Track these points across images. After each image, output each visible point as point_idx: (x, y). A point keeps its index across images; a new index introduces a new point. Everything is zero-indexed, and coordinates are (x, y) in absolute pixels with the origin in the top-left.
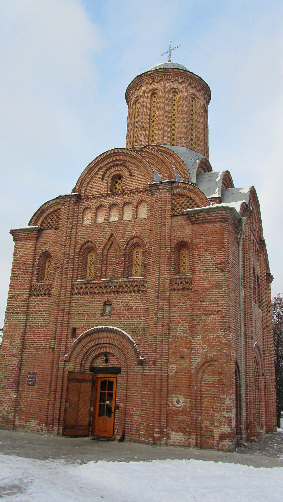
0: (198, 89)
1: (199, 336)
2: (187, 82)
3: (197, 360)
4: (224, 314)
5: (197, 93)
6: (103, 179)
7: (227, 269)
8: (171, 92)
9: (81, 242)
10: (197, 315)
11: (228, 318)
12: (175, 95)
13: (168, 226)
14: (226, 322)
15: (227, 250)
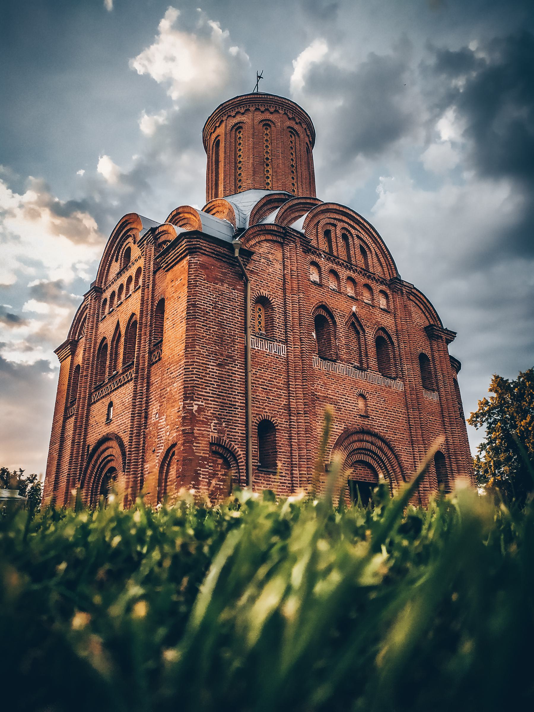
0: (272, 110)
1: (164, 415)
2: (252, 109)
3: (161, 449)
4: (184, 377)
5: (271, 117)
6: (116, 261)
7: (192, 315)
8: (234, 130)
9: (99, 341)
10: (164, 389)
11: (190, 381)
12: (240, 132)
13: (151, 286)
14: (188, 387)
15: (193, 290)
